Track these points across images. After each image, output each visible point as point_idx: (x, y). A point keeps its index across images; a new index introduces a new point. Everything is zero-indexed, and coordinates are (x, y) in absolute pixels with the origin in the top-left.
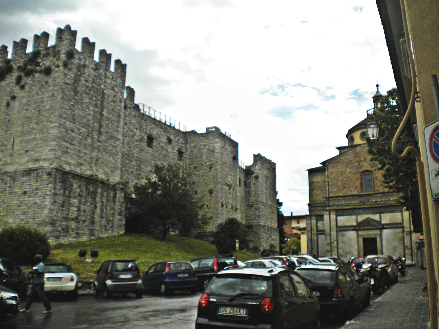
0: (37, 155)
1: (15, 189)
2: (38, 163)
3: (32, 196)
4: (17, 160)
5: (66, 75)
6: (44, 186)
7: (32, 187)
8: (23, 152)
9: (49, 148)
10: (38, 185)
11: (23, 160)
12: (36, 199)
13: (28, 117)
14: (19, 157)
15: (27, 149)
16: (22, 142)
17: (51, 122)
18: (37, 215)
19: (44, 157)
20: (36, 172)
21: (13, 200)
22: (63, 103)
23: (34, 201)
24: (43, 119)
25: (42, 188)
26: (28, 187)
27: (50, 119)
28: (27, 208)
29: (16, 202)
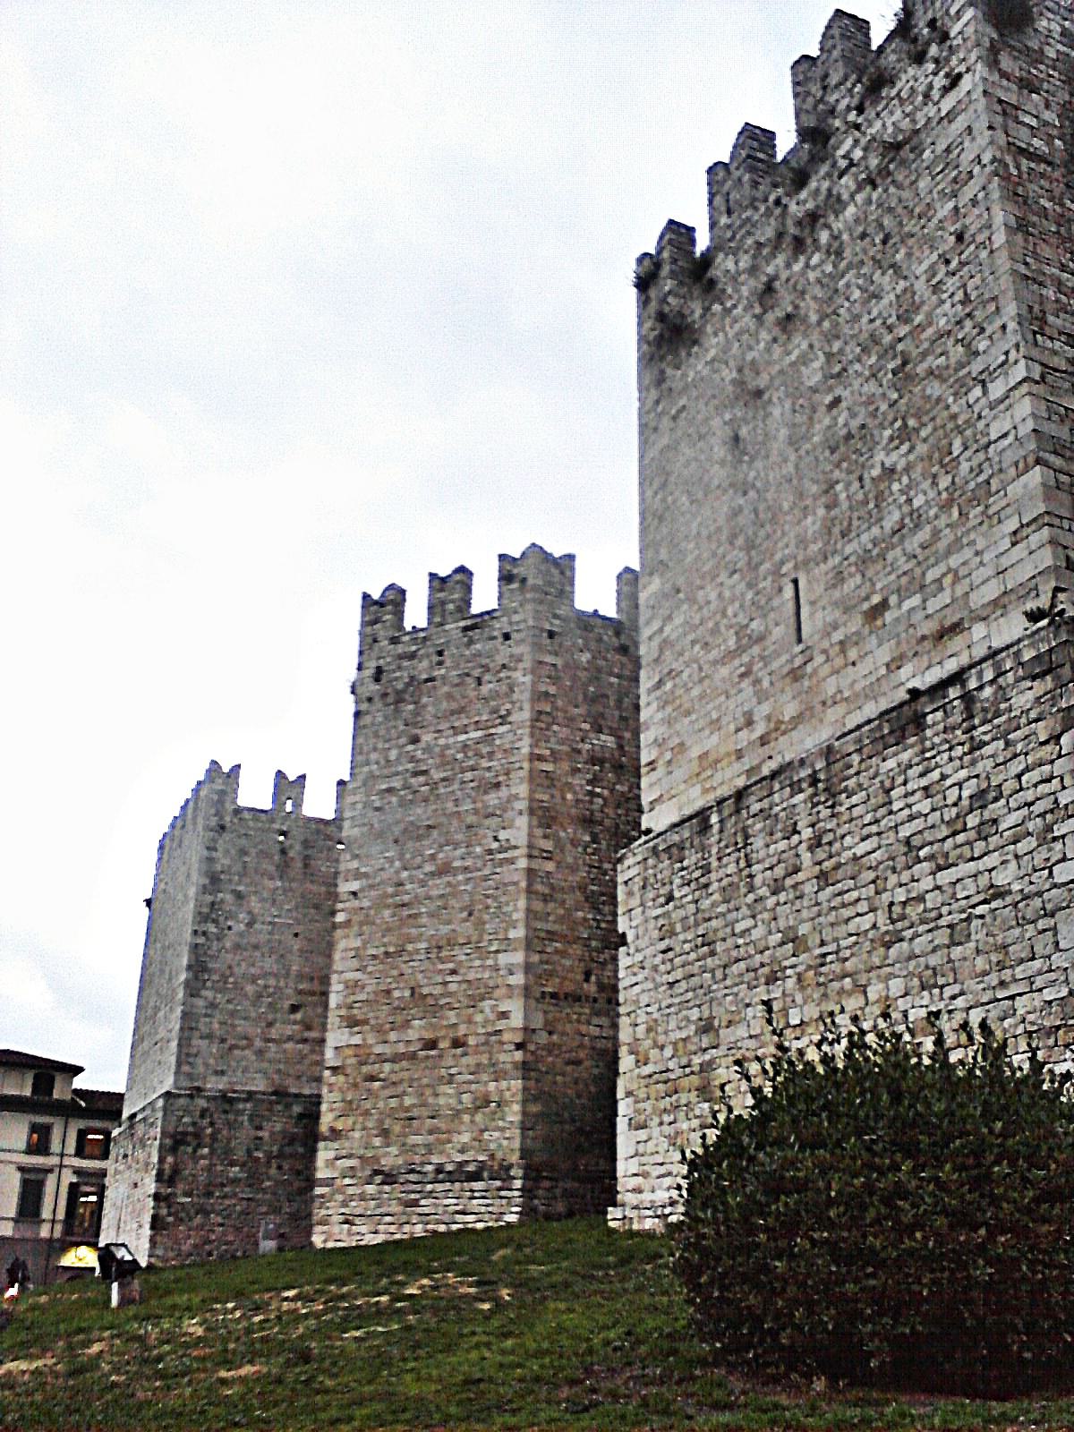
0: (945, 597)
1: (848, 841)
2: (957, 642)
3: (966, 851)
4: (830, 687)
5: (1008, 111)
6: (1030, 759)
7: (952, 795)
8: (855, 623)
9: (1013, 524)
10: (984, 766)
11: (862, 668)
12: (989, 861)
13: (849, 436)
14: (839, 661)
15: (876, 599)
16: (840, 577)
18: (1019, 972)
19: (991, 591)
20: (953, 692)
21: (847, 913)
22: (1035, 255)
23: (983, 881)
24: (935, 389)
25: (1019, 776)
26: (925, 806)
28: (942, 937)
29: (865, 922)
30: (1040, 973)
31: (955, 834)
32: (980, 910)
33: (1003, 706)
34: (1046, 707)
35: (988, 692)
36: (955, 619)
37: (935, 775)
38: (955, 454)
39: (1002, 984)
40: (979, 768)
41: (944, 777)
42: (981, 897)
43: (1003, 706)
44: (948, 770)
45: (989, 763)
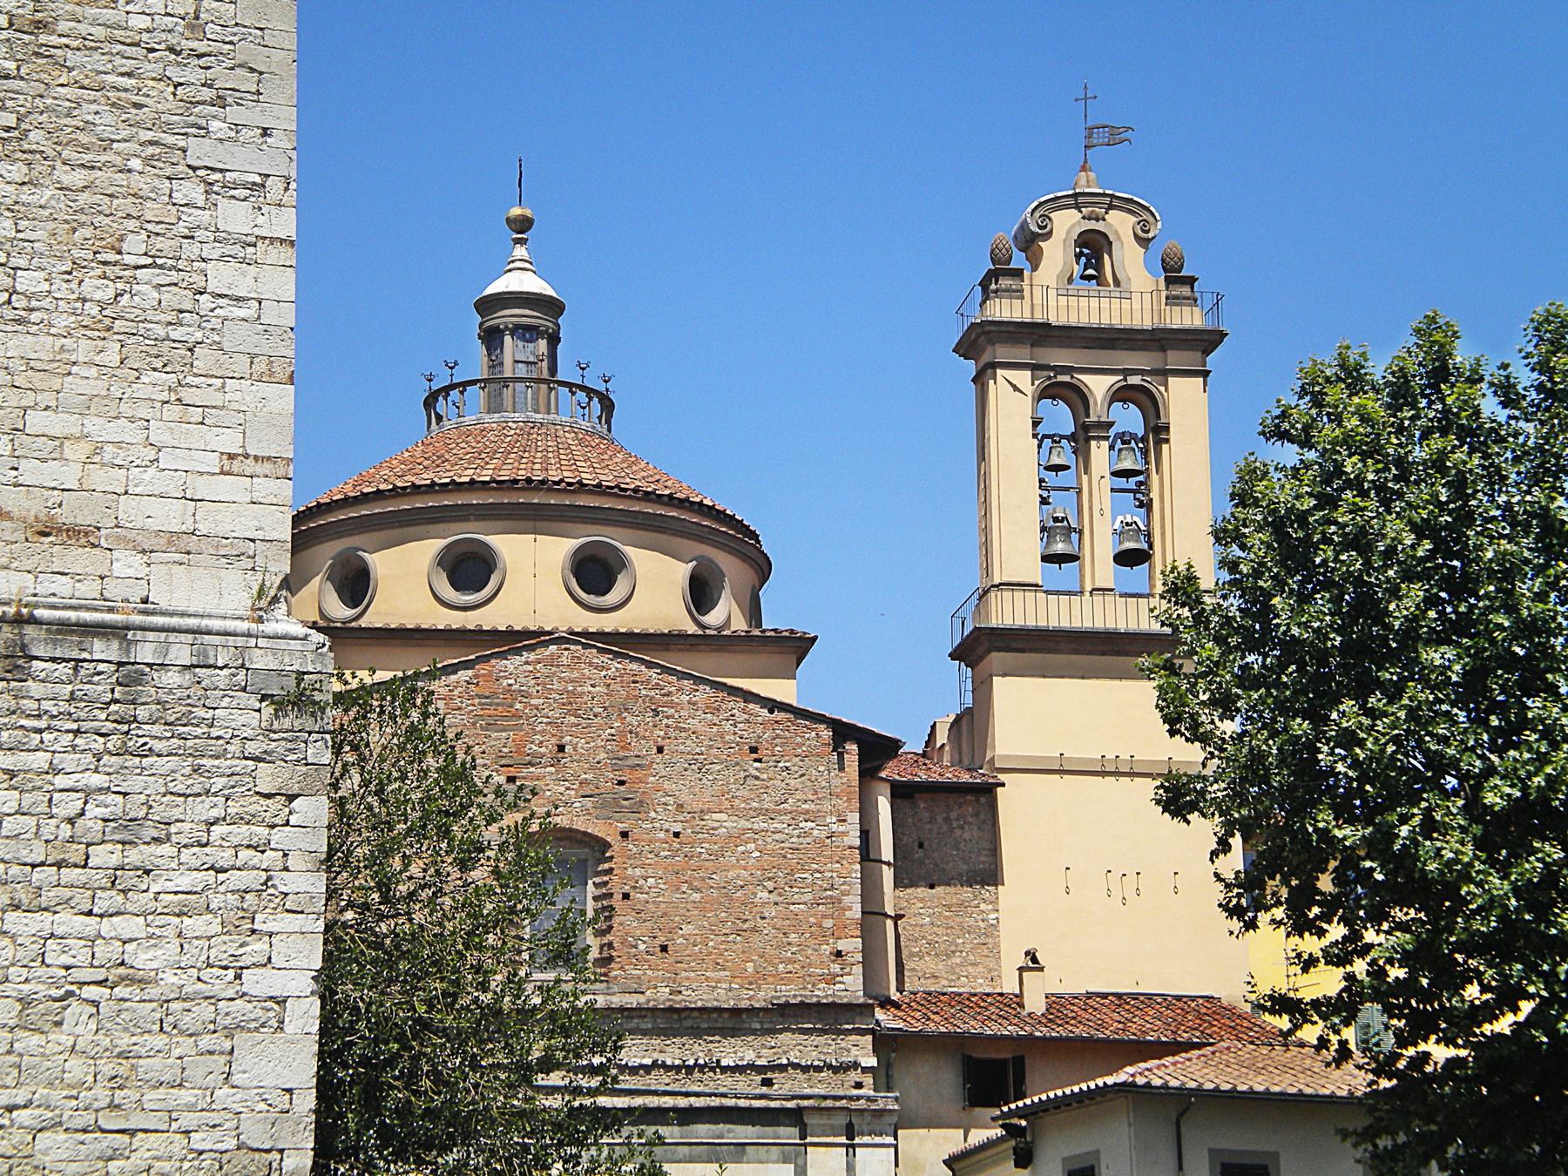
2: (79, 558)
17: (215, 183)
19: (170, 516)
20: (102, 649)
27: (200, 152)
30: (191, 1108)
31: (59, 865)
32: (91, 992)
33: (200, 712)
34: (281, 747)
35: (172, 678)
36: (84, 519)
37: (40, 760)
38: (128, 259)
39: (113, 1107)
40: (134, 783)
41: (55, 770)
42: (100, 974)
43: (200, 712)
44: (68, 761)
45: (157, 785)
